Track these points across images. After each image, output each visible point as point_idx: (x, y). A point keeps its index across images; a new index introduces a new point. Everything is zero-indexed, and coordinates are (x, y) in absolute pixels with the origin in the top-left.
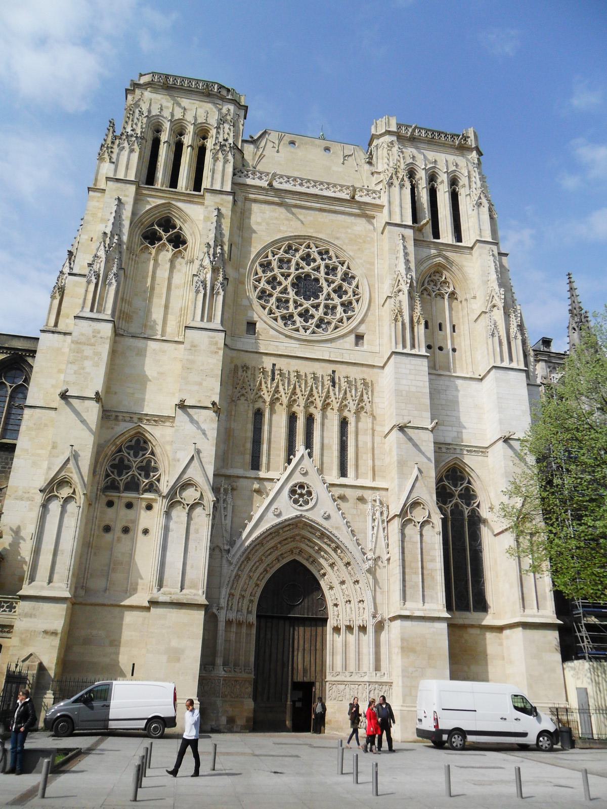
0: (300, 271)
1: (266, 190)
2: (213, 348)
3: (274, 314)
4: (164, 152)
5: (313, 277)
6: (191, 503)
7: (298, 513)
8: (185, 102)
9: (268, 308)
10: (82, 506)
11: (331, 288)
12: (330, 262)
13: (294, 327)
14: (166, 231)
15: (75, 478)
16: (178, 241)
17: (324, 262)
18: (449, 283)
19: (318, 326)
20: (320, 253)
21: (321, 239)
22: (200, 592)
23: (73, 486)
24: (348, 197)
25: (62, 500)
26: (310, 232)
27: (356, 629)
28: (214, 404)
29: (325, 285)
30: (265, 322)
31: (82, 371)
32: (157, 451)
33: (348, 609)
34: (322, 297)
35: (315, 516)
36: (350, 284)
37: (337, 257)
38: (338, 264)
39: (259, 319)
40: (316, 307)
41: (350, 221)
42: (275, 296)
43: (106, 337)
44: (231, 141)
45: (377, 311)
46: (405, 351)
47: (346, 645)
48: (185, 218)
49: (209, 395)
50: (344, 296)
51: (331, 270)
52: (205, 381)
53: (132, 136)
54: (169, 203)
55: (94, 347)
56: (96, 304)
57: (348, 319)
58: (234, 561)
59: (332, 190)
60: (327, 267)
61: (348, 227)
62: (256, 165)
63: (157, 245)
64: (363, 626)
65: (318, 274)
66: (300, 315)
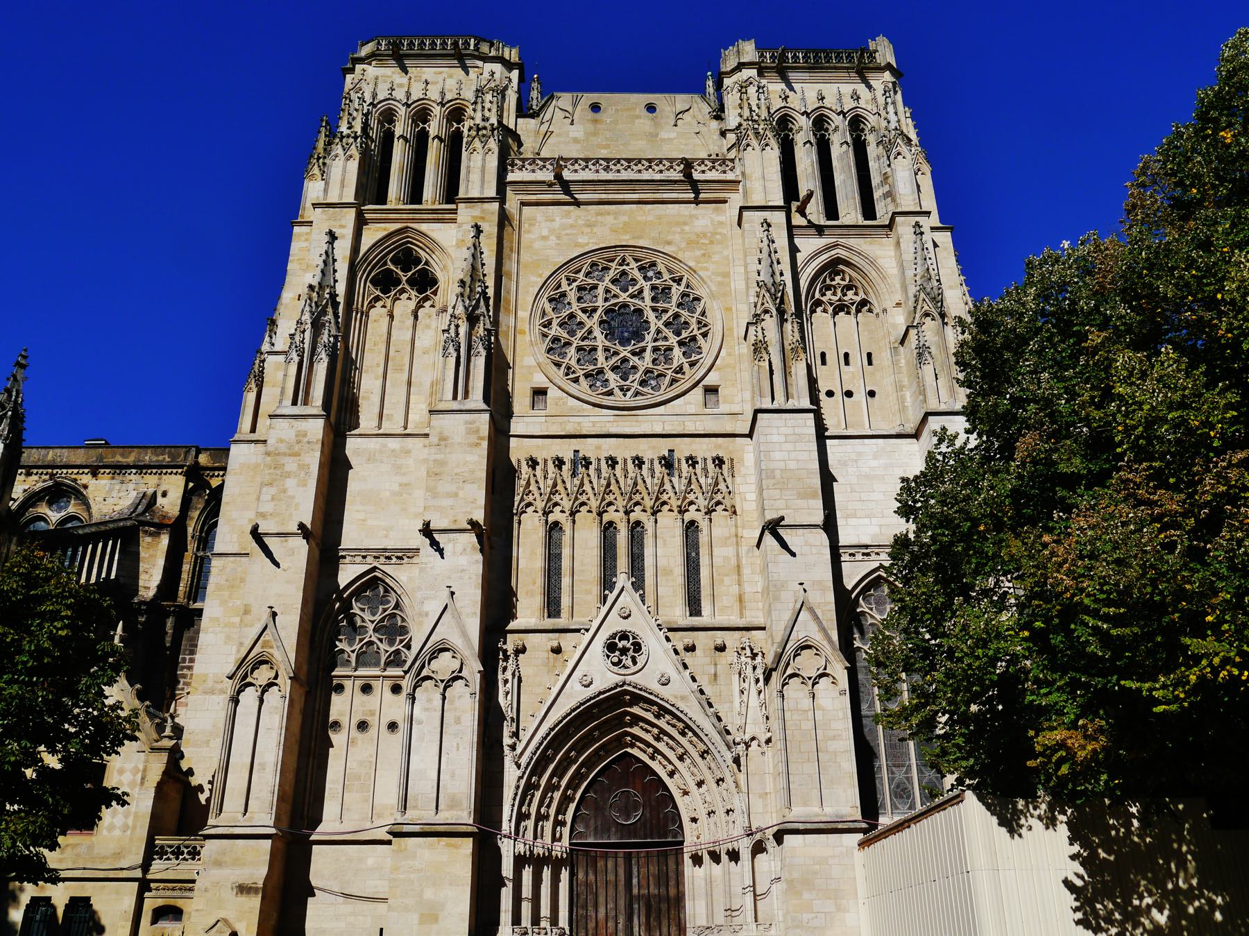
0: (613, 301)
1: (551, 185)
2: (473, 439)
3: (574, 372)
4: (400, 155)
5: (632, 308)
6: (447, 677)
7: (619, 679)
8: (428, 72)
9: (564, 365)
10: (288, 696)
11: (662, 322)
12: (658, 281)
13: (605, 390)
14: (405, 270)
15: (277, 655)
16: (425, 283)
18: (856, 288)
20: (641, 268)
21: (642, 248)
22: (465, 814)
23: (275, 667)
24: (680, 176)
25: (260, 690)
26: (626, 239)
27: (724, 858)
28: (474, 524)
29: (651, 316)
31: (282, 495)
32: (406, 601)
33: (712, 826)
34: (649, 338)
35: (647, 680)
36: (692, 310)
37: (670, 271)
38: (672, 283)
40: (639, 353)
41: (687, 213)
42: (575, 345)
44: (494, 120)
46: (776, 406)
47: (710, 882)
49: (468, 509)
51: (661, 293)
53: (348, 136)
54: (408, 227)
56: (300, 394)
57: (692, 364)
58: (524, 761)
59: (657, 168)
60: (653, 288)
61: (685, 224)
62: (540, 149)
63: (393, 293)
64: (733, 849)
65: (640, 303)
66: (614, 369)
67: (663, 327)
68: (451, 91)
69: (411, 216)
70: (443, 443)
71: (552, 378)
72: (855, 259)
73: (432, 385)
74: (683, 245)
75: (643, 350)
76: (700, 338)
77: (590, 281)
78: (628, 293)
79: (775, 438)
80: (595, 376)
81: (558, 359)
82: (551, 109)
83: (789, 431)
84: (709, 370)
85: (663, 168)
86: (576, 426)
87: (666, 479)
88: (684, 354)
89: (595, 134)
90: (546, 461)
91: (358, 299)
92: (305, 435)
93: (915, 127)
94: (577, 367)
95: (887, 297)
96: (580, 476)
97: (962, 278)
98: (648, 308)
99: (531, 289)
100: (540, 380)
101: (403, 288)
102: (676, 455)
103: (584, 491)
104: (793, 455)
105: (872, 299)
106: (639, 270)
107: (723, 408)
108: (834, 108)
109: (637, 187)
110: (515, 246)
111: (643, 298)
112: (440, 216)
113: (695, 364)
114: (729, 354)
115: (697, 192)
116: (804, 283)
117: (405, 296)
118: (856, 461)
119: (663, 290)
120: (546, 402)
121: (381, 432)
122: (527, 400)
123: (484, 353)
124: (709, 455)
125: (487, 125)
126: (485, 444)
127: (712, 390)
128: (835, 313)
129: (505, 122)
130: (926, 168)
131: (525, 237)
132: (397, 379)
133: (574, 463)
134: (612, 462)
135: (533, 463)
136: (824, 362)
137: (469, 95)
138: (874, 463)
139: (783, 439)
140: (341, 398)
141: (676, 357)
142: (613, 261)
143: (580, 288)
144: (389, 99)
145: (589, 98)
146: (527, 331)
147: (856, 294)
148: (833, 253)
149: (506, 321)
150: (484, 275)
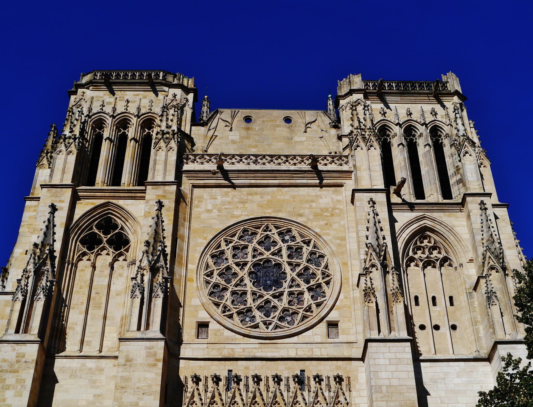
0: (259, 258)
1: (214, 173)
3: (229, 310)
5: (274, 263)
8: (129, 95)
9: (222, 305)
11: (295, 273)
12: (293, 243)
13: (252, 324)
14: (106, 233)
17: (286, 244)
18: (440, 248)
19: (281, 319)
21: (281, 219)
24: (308, 168)
26: (269, 213)
29: (287, 269)
30: (218, 322)
34: (285, 285)
37: (302, 236)
38: (303, 244)
39: (212, 320)
40: (279, 296)
41: (314, 194)
42: (230, 290)
43: (31, 360)
44: (175, 128)
45: (351, 293)
46: (381, 336)
48: (127, 215)
50: (312, 280)
52: (142, 400)
53: (70, 138)
55: (16, 374)
57: (318, 305)
59: (292, 162)
60: (289, 248)
61: (312, 201)
62: (208, 148)
63: (96, 250)
65: (279, 259)
66: (259, 308)
67: (296, 277)
68: (145, 107)
69: (112, 194)
70: (128, 363)
71: (212, 315)
72: (438, 228)
73: (122, 319)
74: (311, 217)
75: (282, 294)
76: (324, 285)
77: (243, 243)
78: (270, 252)
79: (382, 362)
80: (244, 313)
81: (217, 300)
82: (216, 120)
83: (392, 356)
84: (331, 309)
85: (297, 162)
86: (230, 351)
87: (299, 391)
88: (312, 297)
89: (247, 138)
90: (206, 378)
91: (70, 254)
92: (23, 356)
93: (477, 134)
94: (232, 306)
95: (462, 255)
96: (233, 390)
97: (517, 241)
98: (285, 263)
99: (198, 248)
100: (203, 316)
101: (104, 247)
102: (306, 374)
103: (235, 402)
104: (395, 375)
105: (452, 256)
106: (279, 235)
107: (342, 338)
108: (419, 121)
109: (277, 175)
110: (187, 216)
111: (281, 256)
112: (133, 195)
113: (320, 305)
114: (346, 298)
115: (321, 179)
116: (401, 245)
117: (105, 252)
118: (444, 379)
119: (296, 249)
120: (207, 333)
121: (82, 354)
122: (194, 331)
123: (161, 295)
124: (332, 375)
125: (170, 130)
126: (160, 365)
127: (333, 325)
128: (424, 267)
129: (183, 129)
130: (487, 163)
131: (195, 211)
132: (96, 313)
133: (228, 379)
134: (257, 379)
135: (197, 379)
136: (417, 304)
137: (157, 110)
138: (458, 381)
139: (387, 362)
140: (53, 328)
141: (306, 300)
142: (259, 228)
143: (235, 248)
144: (100, 112)
145: (243, 113)
146: (195, 279)
147: (440, 253)
148: (421, 223)
149: (180, 271)
150: (164, 238)
